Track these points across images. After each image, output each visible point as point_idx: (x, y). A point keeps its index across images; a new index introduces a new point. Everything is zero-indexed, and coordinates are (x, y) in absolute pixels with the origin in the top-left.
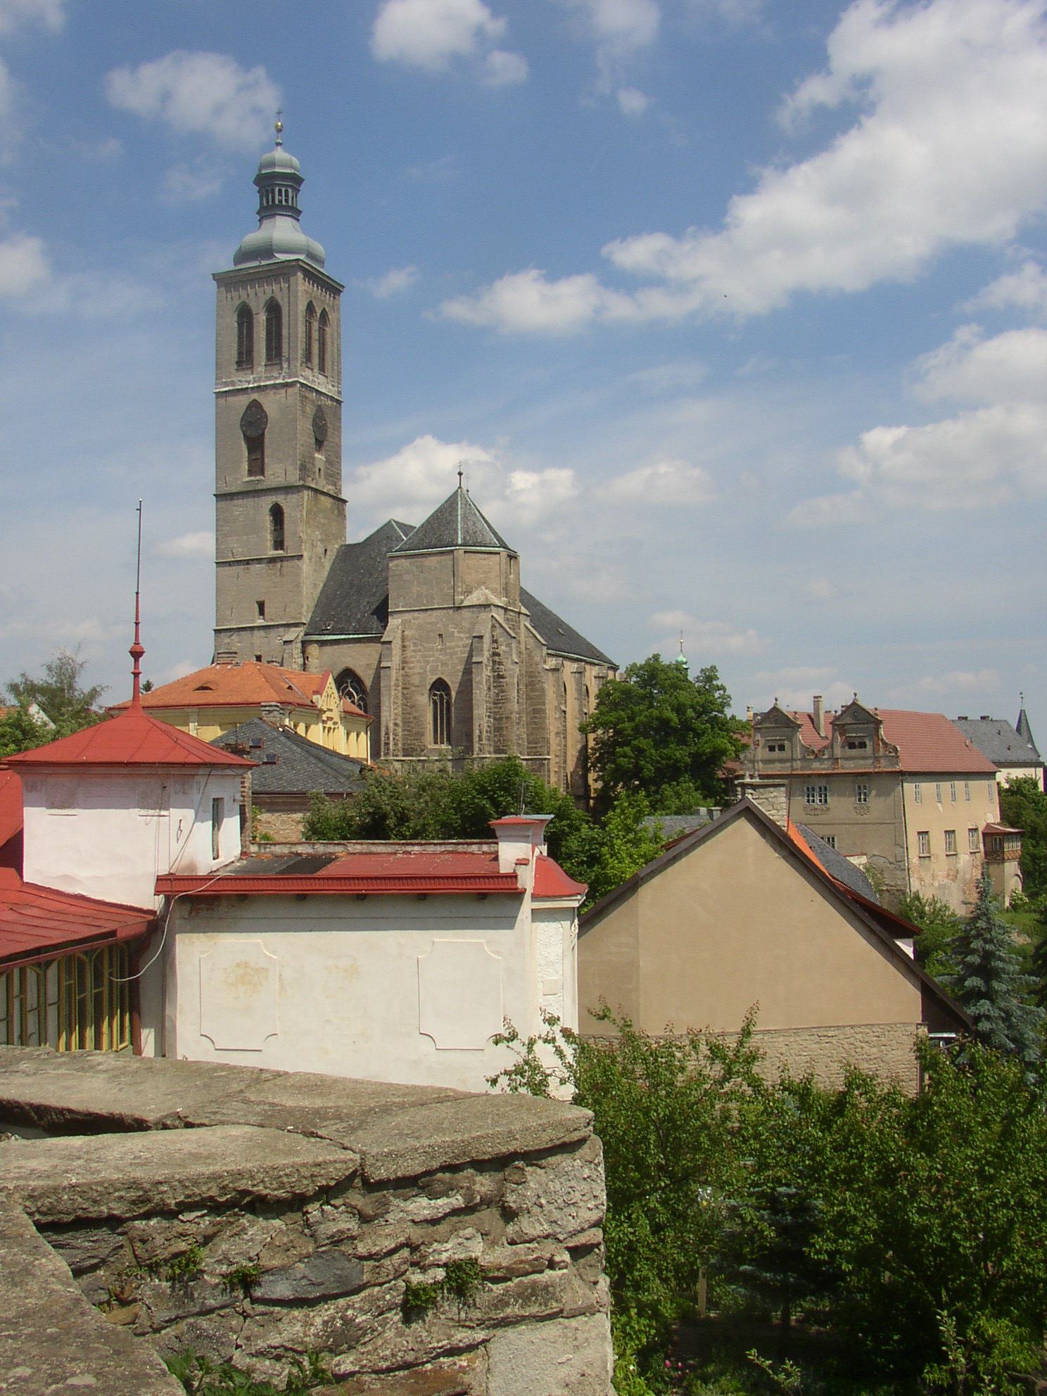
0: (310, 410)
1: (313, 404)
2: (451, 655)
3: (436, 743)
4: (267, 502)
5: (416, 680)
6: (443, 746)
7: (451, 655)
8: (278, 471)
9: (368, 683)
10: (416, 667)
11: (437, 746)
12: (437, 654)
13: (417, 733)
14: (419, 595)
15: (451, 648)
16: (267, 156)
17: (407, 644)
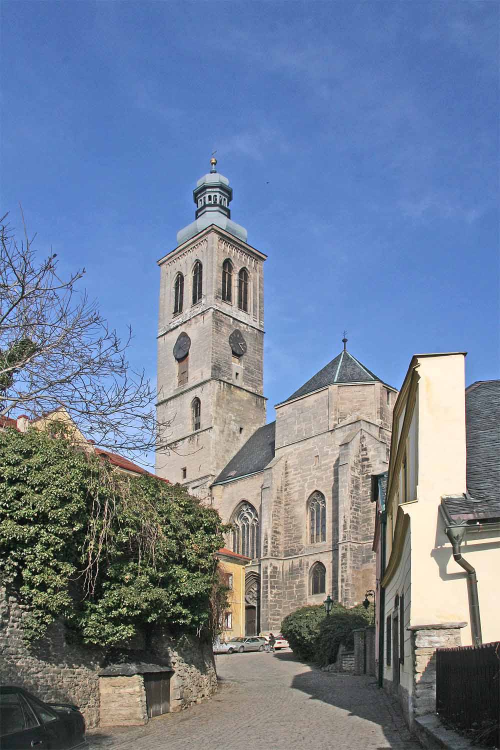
0: (226, 332)
1: (229, 326)
2: (326, 470)
3: (312, 542)
4: (189, 399)
5: (295, 496)
6: (318, 543)
7: (326, 470)
8: (199, 371)
9: (257, 508)
10: (295, 487)
11: (313, 545)
12: (313, 472)
13: (296, 538)
14: (299, 431)
15: (325, 464)
16: (199, 184)
17: (289, 470)
